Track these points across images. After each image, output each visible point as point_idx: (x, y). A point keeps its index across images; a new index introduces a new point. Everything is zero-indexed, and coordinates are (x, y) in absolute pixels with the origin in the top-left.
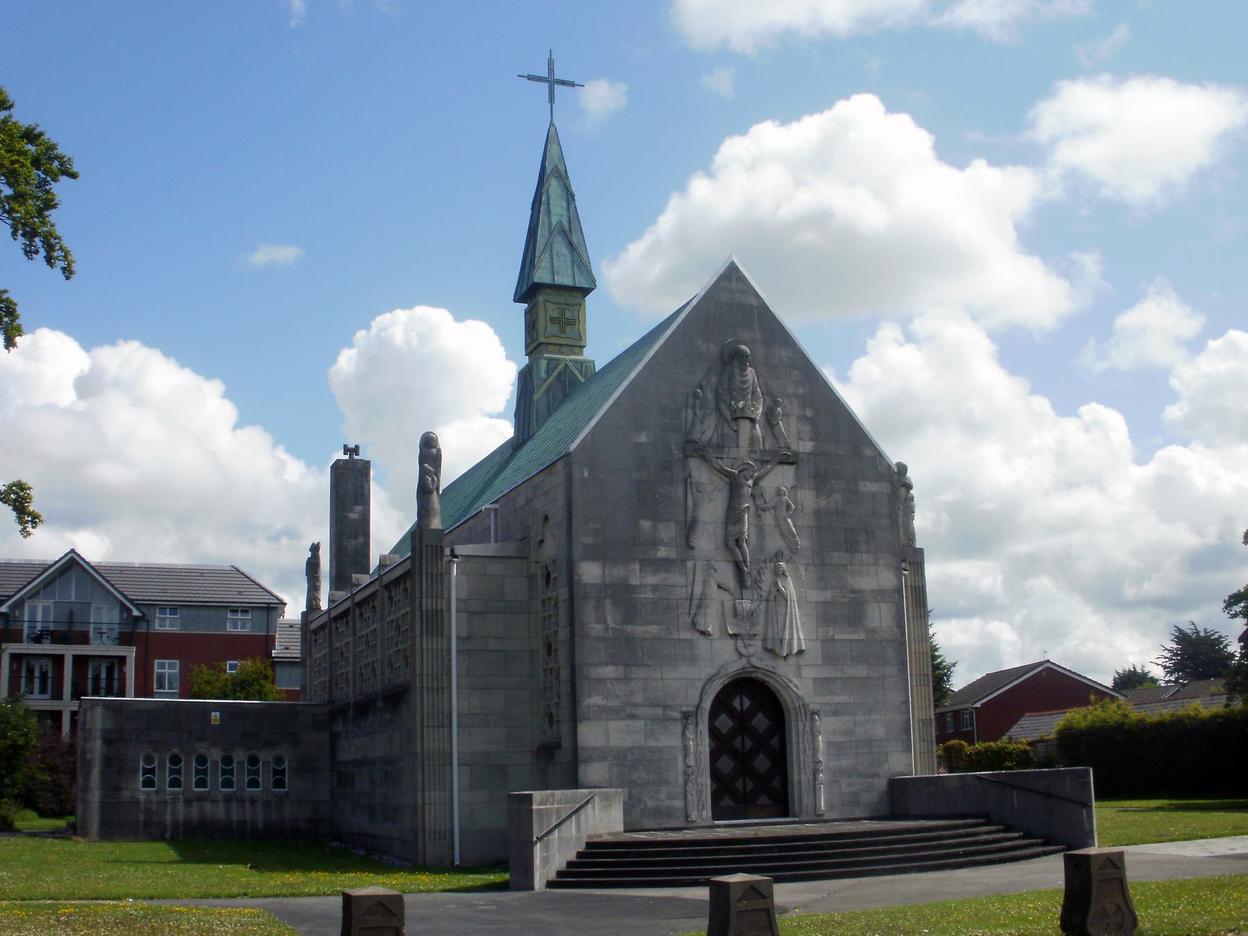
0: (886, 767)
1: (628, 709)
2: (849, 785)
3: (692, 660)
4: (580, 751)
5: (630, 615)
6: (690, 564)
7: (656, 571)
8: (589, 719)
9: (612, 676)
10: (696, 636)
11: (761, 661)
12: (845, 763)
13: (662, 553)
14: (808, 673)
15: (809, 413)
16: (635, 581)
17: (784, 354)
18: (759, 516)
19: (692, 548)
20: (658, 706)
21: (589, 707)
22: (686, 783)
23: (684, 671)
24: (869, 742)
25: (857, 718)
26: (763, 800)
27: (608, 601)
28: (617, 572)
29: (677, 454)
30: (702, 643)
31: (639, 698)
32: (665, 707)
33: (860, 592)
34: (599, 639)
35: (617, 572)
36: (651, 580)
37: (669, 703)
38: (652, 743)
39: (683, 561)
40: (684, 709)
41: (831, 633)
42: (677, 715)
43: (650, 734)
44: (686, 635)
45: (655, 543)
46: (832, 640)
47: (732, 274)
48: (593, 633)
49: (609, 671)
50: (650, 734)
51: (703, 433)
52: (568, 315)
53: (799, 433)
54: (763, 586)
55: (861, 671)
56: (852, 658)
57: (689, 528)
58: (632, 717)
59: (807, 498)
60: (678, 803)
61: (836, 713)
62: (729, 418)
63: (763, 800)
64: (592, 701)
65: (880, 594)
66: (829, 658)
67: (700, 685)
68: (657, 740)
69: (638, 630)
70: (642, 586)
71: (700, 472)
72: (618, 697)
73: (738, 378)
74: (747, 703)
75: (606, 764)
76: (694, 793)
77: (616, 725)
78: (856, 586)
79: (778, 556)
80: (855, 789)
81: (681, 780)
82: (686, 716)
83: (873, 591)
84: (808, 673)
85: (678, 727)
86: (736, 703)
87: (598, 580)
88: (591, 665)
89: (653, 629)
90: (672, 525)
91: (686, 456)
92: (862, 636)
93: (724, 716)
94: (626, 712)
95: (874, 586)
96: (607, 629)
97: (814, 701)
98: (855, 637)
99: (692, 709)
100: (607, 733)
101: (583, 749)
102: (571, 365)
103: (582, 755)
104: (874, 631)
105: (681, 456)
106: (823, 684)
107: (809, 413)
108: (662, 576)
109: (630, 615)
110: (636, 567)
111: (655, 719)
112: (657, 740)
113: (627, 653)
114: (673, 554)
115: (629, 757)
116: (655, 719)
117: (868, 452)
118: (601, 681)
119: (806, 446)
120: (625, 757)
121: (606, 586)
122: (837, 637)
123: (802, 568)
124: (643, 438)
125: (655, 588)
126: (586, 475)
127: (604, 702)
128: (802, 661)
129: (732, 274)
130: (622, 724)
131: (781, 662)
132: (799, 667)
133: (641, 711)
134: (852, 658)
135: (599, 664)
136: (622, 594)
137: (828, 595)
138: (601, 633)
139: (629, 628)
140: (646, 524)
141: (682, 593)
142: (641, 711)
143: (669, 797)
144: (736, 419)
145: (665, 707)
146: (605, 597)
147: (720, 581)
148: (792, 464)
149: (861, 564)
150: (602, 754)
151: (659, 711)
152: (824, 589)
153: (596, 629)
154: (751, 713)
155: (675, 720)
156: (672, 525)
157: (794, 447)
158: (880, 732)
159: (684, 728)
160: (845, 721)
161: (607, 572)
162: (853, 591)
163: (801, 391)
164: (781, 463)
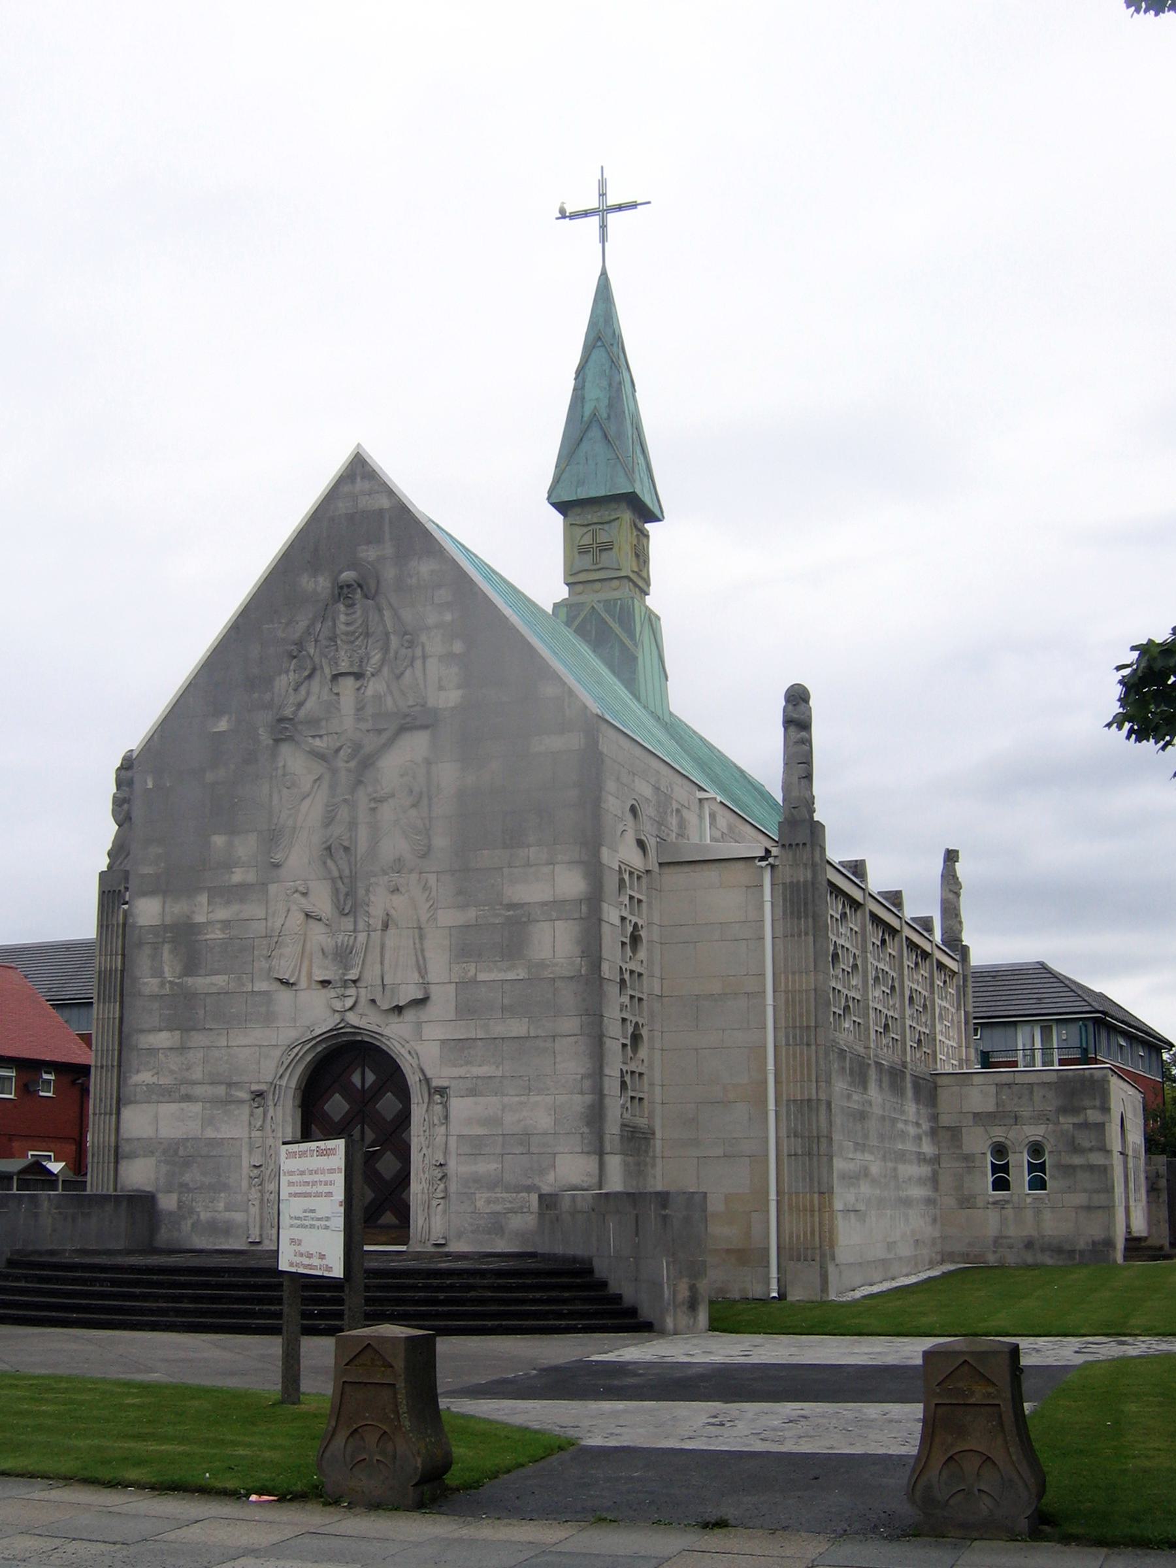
0: (551, 1177)
1: (182, 1087)
2: (488, 1202)
3: (269, 1019)
4: (122, 1143)
5: (191, 967)
6: (273, 888)
7: (228, 902)
8: (135, 1102)
9: (168, 1044)
10: (276, 986)
11: (365, 1020)
12: (486, 1167)
13: (238, 876)
14: (435, 1032)
15: (458, 647)
16: (200, 918)
17: (425, 568)
18: (374, 809)
19: (277, 866)
20: (221, 1083)
21: (136, 1085)
22: (250, 1188)
23: (257, 1035)
24: (525, 1137)
25: (506, 1099)
26: (388, 1218)
27: (166, 948)
28: (177, 909)
29: (265, 738)
30: (284, 997)
31: (197, 1074)
32: (230, 1085)
33: (522, 905)
34: (154, 997)
35: (177, 909)
36: (222, 914)
37: (235, 1079)
38: (210, 1133)
39: (264, 885)
40: (255, 1087)
41: (472, 972)
42: (244, 1095)
43: (209, 1121)
44: (262, 986)
45: (228, 865)
46: (474, 981)
47: (359, 470)
48: (147, 991)
49: (163, 1039)
50: (209, 1121)
51: (300, 705)
52: (603, 538)
53: (440, 680)
54: (371, 910)
55: (517, 1027)
56: (503, 1009)
57: (273, 838)
58: (187, 1098)
59: (448, 775)
60: (239, 1217)
61: (473, 1092)
62: (329, 677)
63: (388, 1218)
64: (142, 1077)
65: (556, 908)
66: (466, 1010)
67: (277, 1053)
68: (218, 1130)
69: (200, 983)
70: (209, 923)
71: (293, 760)
72: (172, 1072)
73: (343, 618)
74: (370, 1078)
75: (151, 1161)
76: (257, 1203)
77: (168, 1109)
78: (515, 901)
79: (398, 866)
80: (498, 1208)
81: (245, 1184)
82: (259, 1095)
83: (544, 904)
84: (435, 1032)
85: (246, 1109)
86: (356, 1079)
87: (156, 922)
88: (142, 1031)
89: (220, 980)
90: (252, 839)
91: (277, 741)
92: (522, 974)
93: (337, 1095)
94: (178, 1093)
95: (547, 896)
96: (162, 985)
97: (441, 1075)
98: (511, 976)
99: (263, 1087)
100: (156, 1118)
101: (128, 1140)
102: (600, 608)
103: (125, 1148)
104: (542, 965)
105: (271, 742)
106: (457, 1048)
107: (458, 647)
108: (235, 907)
109: (191, 967)
110: (203, 898)
111: (216, 1102)
112: (218, 1130)
113: (185, 1012)
114: (251, 877)
115: (181, 1153)
116: (216, 1102)
117: (549, 690)
118: (153, 1051)
119: (449, 698)
120: (176, 1152)
121: (165, 927)
122: (482, 977)
123: (432, 879)
124: (223, 725)
125: (226, 924)
126: (150, 785)
127: (155, 1079)
128: (426, 1013)
129: (359, 470)
130: (174, 1107)
131: (394, 1018)
132: (419, 1025)
133: (199, 1091)
134: (503, 1009)
135: (149, 1031)
136: (183, 937)
137: (471, 914)
138: (156, 990)
139: (190, 981)
140: (219, 840)
141: (259, 928)
142: (199, 1091)
143: (228, 1209)
144: (335, 677)
145: (230, 1085)
146: (163, 943)
147: (309, 908)
148: (426, 727)
149: (528, 864)
150: (149, 1147)
151: (221, 1090)
152: (464, 907)
153: (150, 984)
154: (377, 1092)
155: (243, 1102)
156: (252, 839)
157: (431, 703)
158: (544, 1121)
159: (252, 1115)
160: (487, 1104)
161: (167, 909)
162: (512, 906)
163: (448, 617)
164: (402, 729)
